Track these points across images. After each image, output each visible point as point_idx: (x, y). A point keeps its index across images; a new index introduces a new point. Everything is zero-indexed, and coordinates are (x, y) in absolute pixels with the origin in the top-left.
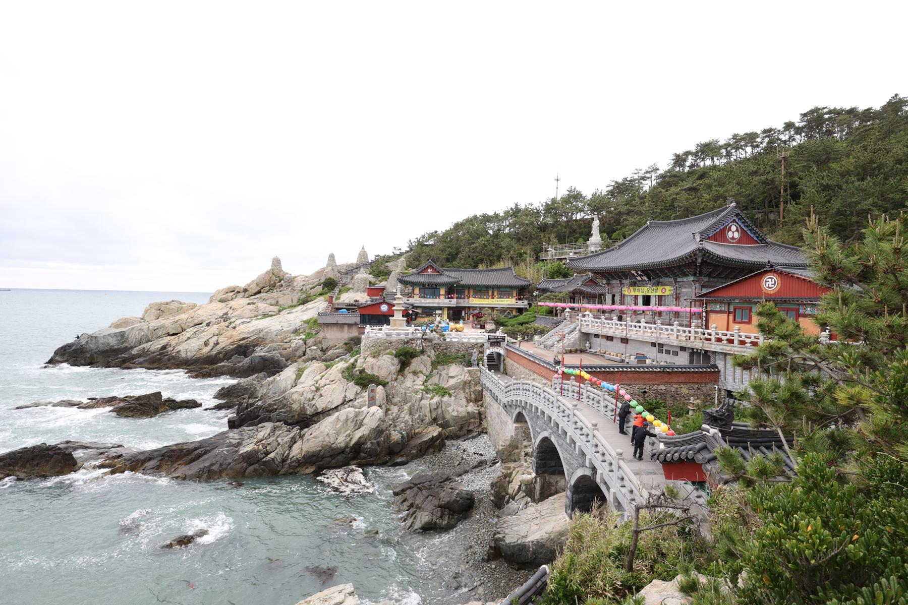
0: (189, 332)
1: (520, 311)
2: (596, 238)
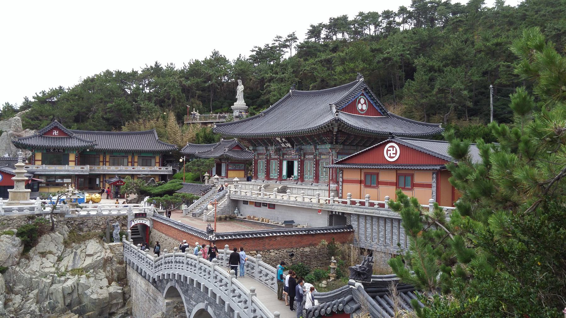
1: (163, 178)
2: (240, 103)
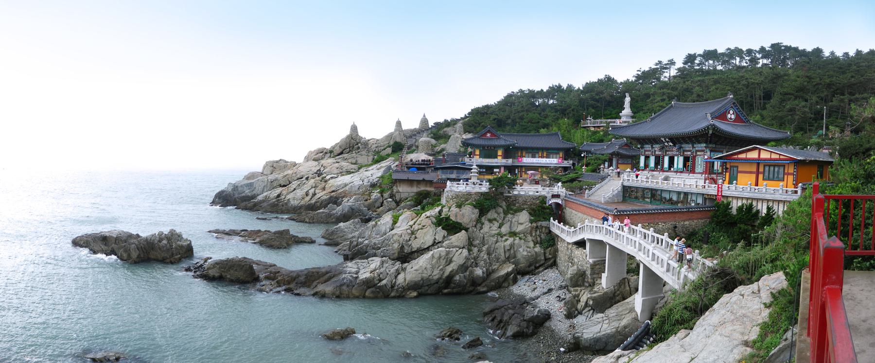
0: (294, 184)
